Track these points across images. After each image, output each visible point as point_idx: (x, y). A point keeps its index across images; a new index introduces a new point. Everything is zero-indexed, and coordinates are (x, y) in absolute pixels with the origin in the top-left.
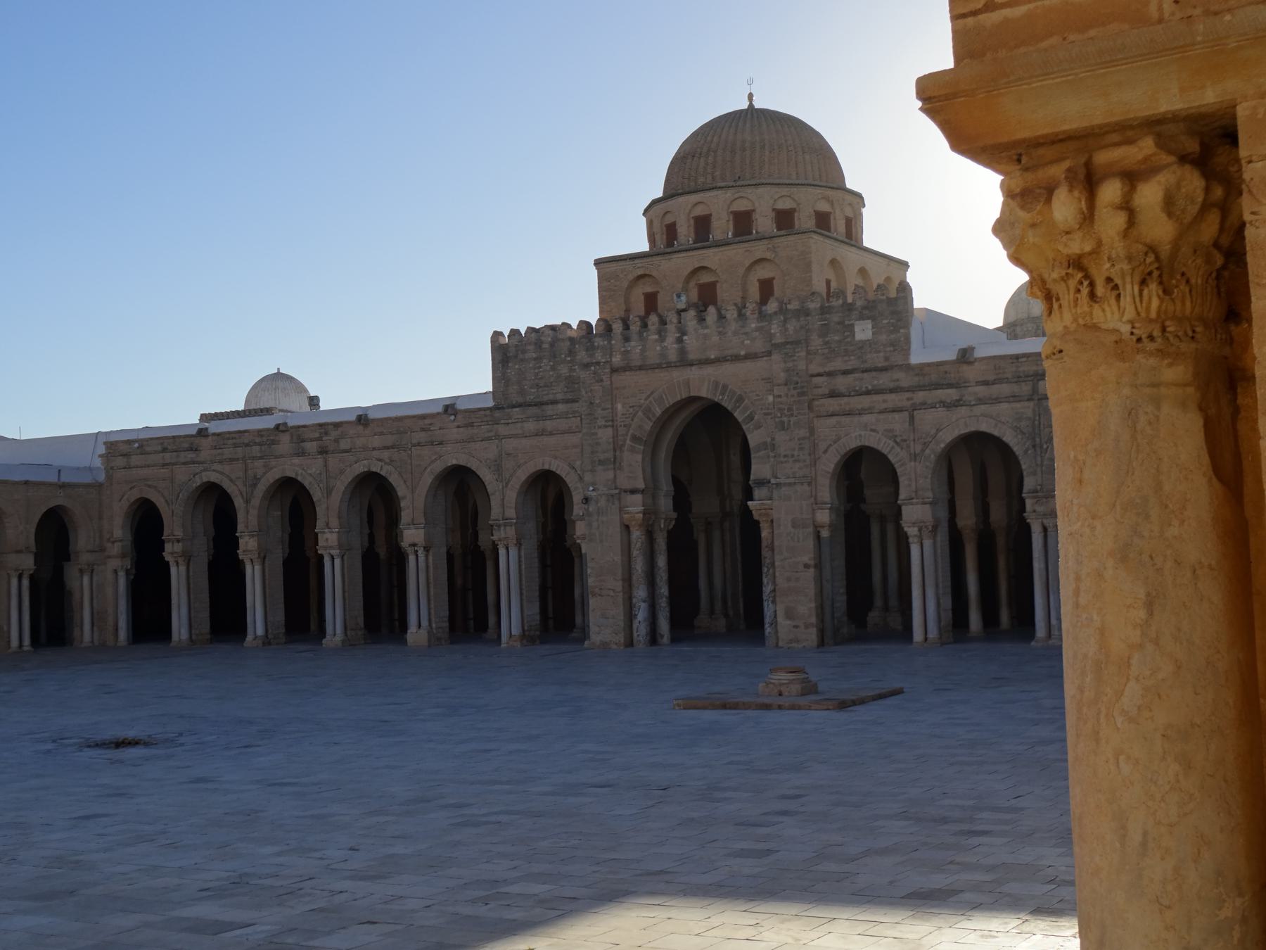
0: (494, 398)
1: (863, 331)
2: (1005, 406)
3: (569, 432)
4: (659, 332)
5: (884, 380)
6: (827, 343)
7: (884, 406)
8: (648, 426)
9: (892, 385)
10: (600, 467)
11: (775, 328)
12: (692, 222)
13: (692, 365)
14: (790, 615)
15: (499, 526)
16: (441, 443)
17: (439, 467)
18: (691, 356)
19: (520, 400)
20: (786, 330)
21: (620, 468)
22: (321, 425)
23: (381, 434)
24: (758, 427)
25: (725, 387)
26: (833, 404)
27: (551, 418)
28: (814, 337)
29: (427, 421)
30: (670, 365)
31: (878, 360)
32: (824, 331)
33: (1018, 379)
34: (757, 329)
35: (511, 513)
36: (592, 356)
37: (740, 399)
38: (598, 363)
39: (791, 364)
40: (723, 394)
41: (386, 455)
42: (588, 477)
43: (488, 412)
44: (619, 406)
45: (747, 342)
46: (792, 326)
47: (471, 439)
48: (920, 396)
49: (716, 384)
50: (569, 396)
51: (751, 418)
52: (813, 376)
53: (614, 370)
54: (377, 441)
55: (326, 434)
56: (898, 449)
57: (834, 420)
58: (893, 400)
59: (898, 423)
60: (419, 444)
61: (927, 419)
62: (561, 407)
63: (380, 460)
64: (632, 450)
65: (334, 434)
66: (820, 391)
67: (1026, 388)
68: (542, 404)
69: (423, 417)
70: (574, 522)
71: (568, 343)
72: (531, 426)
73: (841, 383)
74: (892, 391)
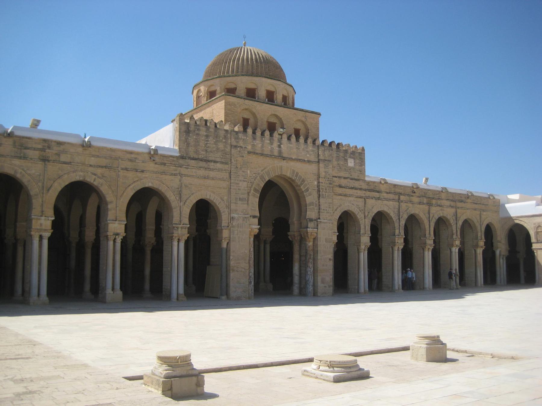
0: (180, 151)
1: (351, 163)
2: (391, 203)
3: (222, 179)
4: (270, 140)
5: (356, 184)
6: (338, 164)
7: (357, 195)
8: (262, 185)
9: (360, 187)
10: (240, 202)
11: (320, 153)
12: (265, 92)
13: (284, 159)
14: (323, 282)
15: (178, 228)
16: (143, 171)
17: (139, 186)
18: (284, 156)
19: (196, 157)
20: (325, 154)
21: (248, 204)
22: (45, 140)
23: (98, 156)
24: (310, 195)
25: (297, 174)
26: (339, 190)
27: (213, 170)
28: (334, 160)
29: (133, 156)
30: (276, 157)
31: (355, 176)
32: (338, 158)
33: (395, 193)
34: (313, 151)
35: (186, 220)
36: (237, 142)
37: (303, 181)
38: (241, 147)
39: (327, 170)
40: (296, 176)
41: (99, 171)
42: (233, 207)
43: (175, 159)
44: (249, 172)
45: (308, 155)
46: (327, 153)
47: (163, 173)
48: (368, 194)
49: (294, 171)
50: (223, 160)
51: (307, 190)
52: (333, 177)
53: (249, 153)
54: (93, 161)
55: (49, 148)
56: (360, 213)
57: (340, 197)
58: (359, 193)
59: (361, 202)
60: (126, 169)
61: (370, 202)
62: (219, 166)
63: (95, 175)
64: (254, 196)
65: (56, 149)
66: (335, 184)
67: (397, 197)
68: (209, 161)
69: (131, 153)
70: (222, 230)
71: (224, 132)
72: (202, 172)
73: (343, 182)
74: (361, 189)
